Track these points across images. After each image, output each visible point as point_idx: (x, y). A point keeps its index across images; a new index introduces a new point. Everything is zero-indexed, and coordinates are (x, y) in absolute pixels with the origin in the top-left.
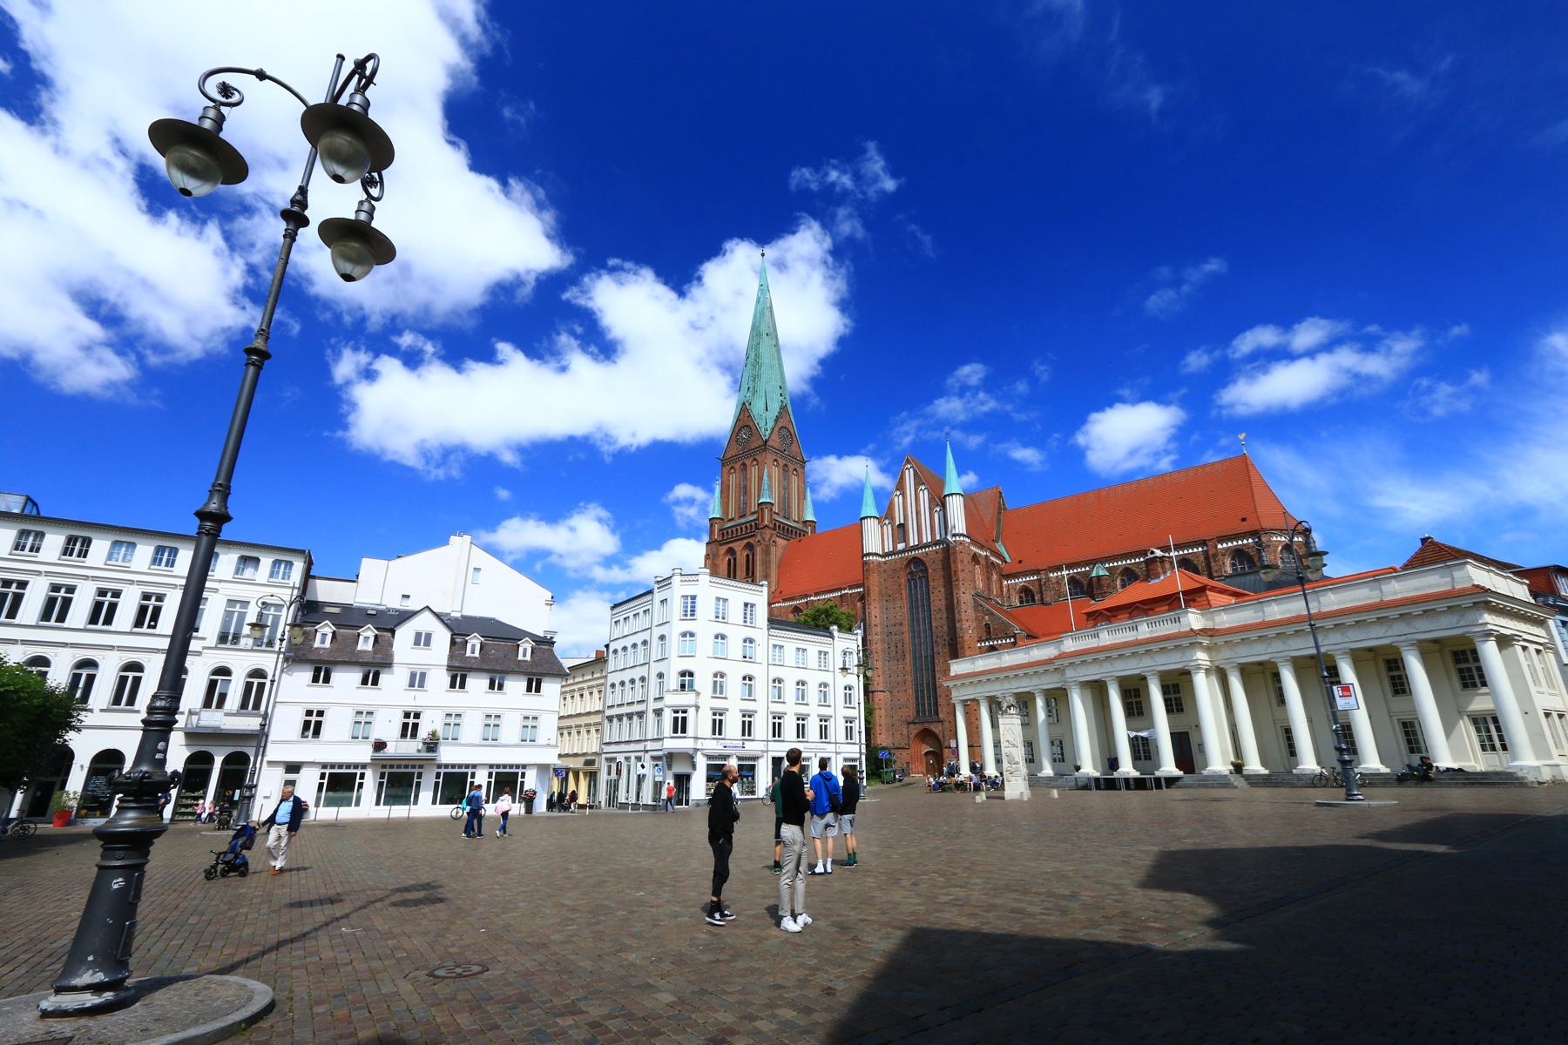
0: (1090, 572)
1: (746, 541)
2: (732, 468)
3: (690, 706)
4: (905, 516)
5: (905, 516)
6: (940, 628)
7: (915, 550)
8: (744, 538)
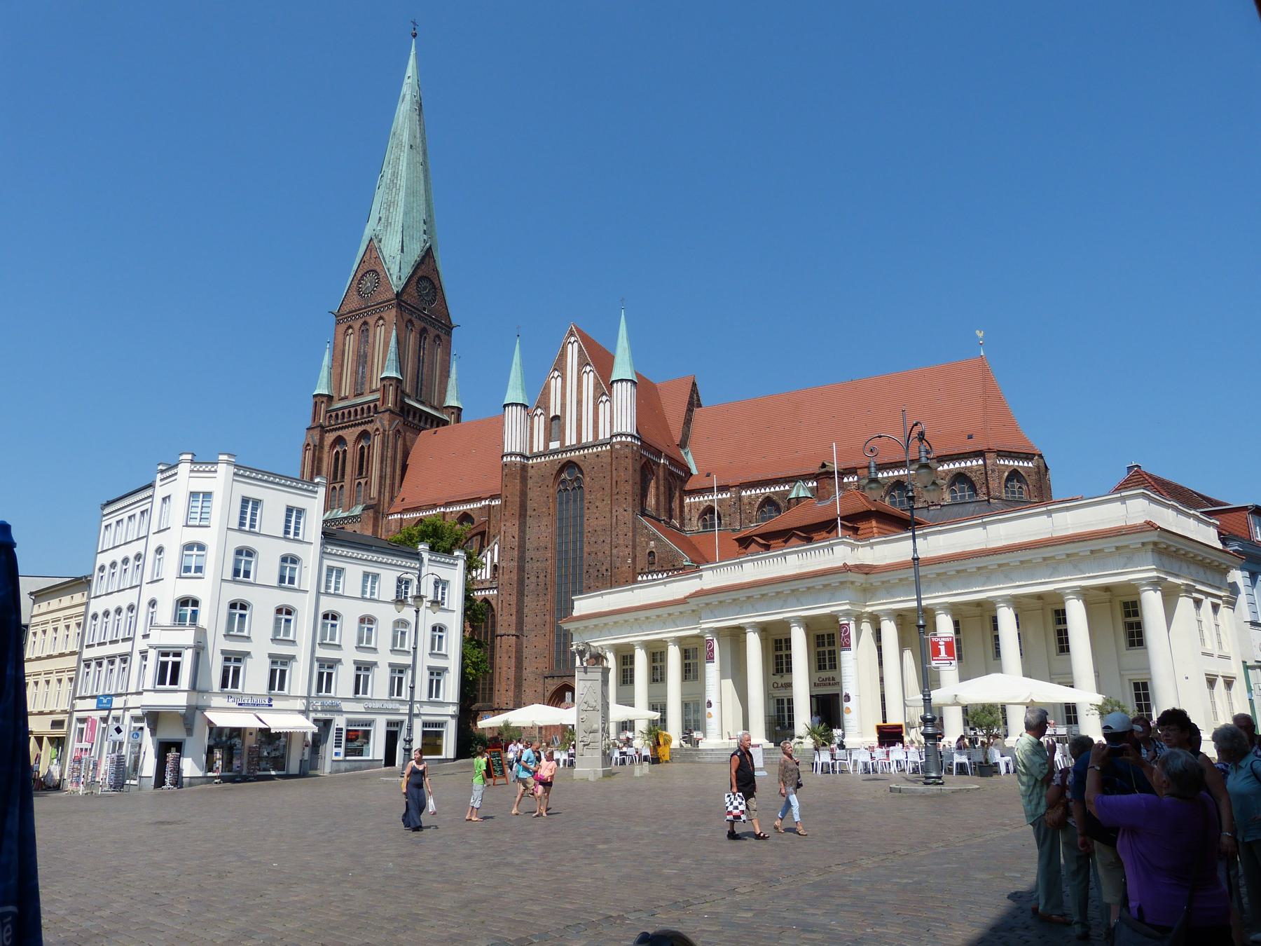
6: (593, 555)
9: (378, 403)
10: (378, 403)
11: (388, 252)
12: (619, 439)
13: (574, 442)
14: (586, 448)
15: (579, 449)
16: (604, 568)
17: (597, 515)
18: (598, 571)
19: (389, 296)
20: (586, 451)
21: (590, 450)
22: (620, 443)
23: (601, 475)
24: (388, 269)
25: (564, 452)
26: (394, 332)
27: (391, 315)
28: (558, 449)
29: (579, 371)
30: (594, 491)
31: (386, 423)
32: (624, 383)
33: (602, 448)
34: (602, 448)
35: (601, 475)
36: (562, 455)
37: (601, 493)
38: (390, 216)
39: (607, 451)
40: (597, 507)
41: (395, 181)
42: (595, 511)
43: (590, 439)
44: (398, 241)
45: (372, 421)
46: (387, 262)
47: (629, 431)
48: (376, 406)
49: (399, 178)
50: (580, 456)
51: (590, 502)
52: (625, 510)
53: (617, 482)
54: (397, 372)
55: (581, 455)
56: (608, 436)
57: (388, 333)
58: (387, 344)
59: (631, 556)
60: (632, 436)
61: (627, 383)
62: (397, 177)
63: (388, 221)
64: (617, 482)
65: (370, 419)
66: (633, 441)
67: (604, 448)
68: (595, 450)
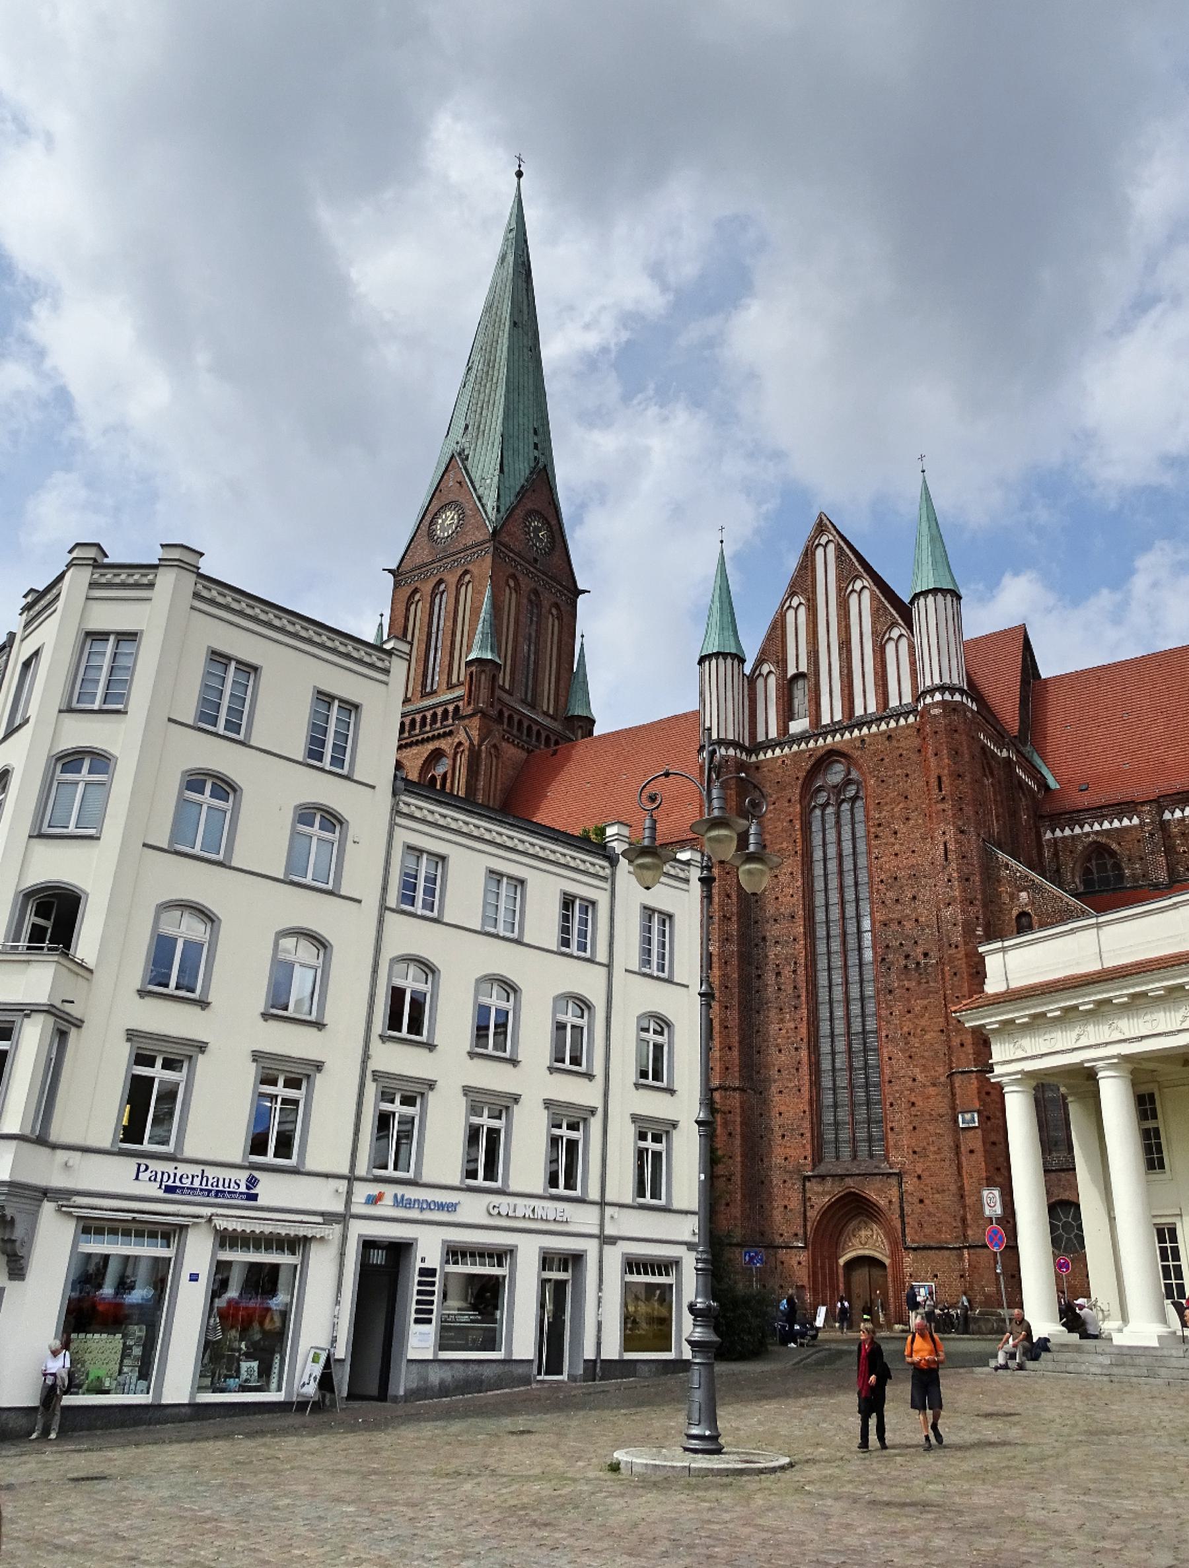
1: (430, 747)
3: (27, 1011)
8: (428, 740)
9: (461, 704)
10: (461, 704)
11: (479, 473)
12: (938, 697)
13: (838, 717)
14: (864, 724)
15: (849, 727)
16: (920, 950)
17: (897, 847)
18: (907, 957)
19: (480, 536)
20: (865, 730)
21: (874, 729)
22: (943, 703)
23: (898, 772)
24: (480, 498)
25: (820, 735)
26: (488, 593)
27: (483, 567)
28: (807, 731)
29: (840, 590)
30: (886, 804)
31: (475, 734)
32: (930, 598)
33: (897, 721)
34: (897, 721)
35: (898, 772)
36: (816, 741)
37: (901, 805)
38: (483, 421)
39: (908, 726)
40: (896, 833)
41: (490, 373)
42: (892, 840)
43: (872, 708)
44: (494, 456)
45: (451, 733)
46: (477, 487)
47: (956, 681)
48: (457, 708)
49: (497, 367)
50: (852, 740)
51: (879, 825)
52: (962, 832)
53: (939, 778)
54: (492, 651)
55: (856, 738)
56: (907, 699)
57: (478, 593)
58: (476, 612)
59: (981, 921)
60: (962, 691)
61: (945, 597)
62: (494, 367)
63: (479, 427)
64: (939, 778)
65: (447, 730)
66: (965, 700)
67: (902, 722)
68: (883, 727)
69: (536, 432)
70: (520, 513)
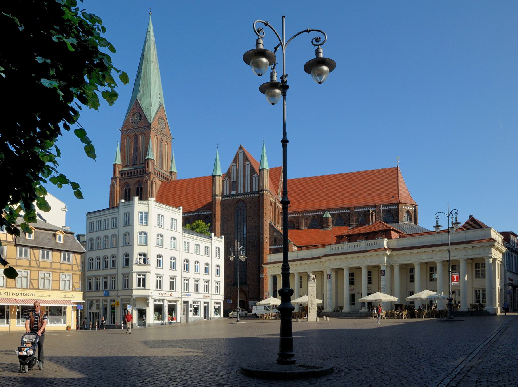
0: (323, 215)
2: (128, 136)
4: (237, 177)
5: (237, 177)
7: (241, 195)
69: (159, 94)
70: (157, 117)
